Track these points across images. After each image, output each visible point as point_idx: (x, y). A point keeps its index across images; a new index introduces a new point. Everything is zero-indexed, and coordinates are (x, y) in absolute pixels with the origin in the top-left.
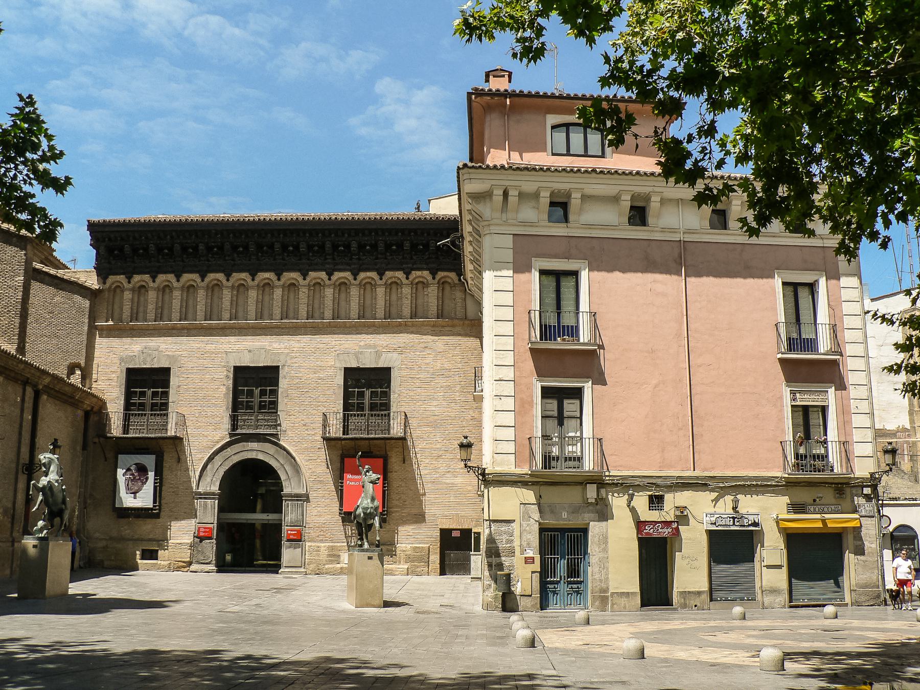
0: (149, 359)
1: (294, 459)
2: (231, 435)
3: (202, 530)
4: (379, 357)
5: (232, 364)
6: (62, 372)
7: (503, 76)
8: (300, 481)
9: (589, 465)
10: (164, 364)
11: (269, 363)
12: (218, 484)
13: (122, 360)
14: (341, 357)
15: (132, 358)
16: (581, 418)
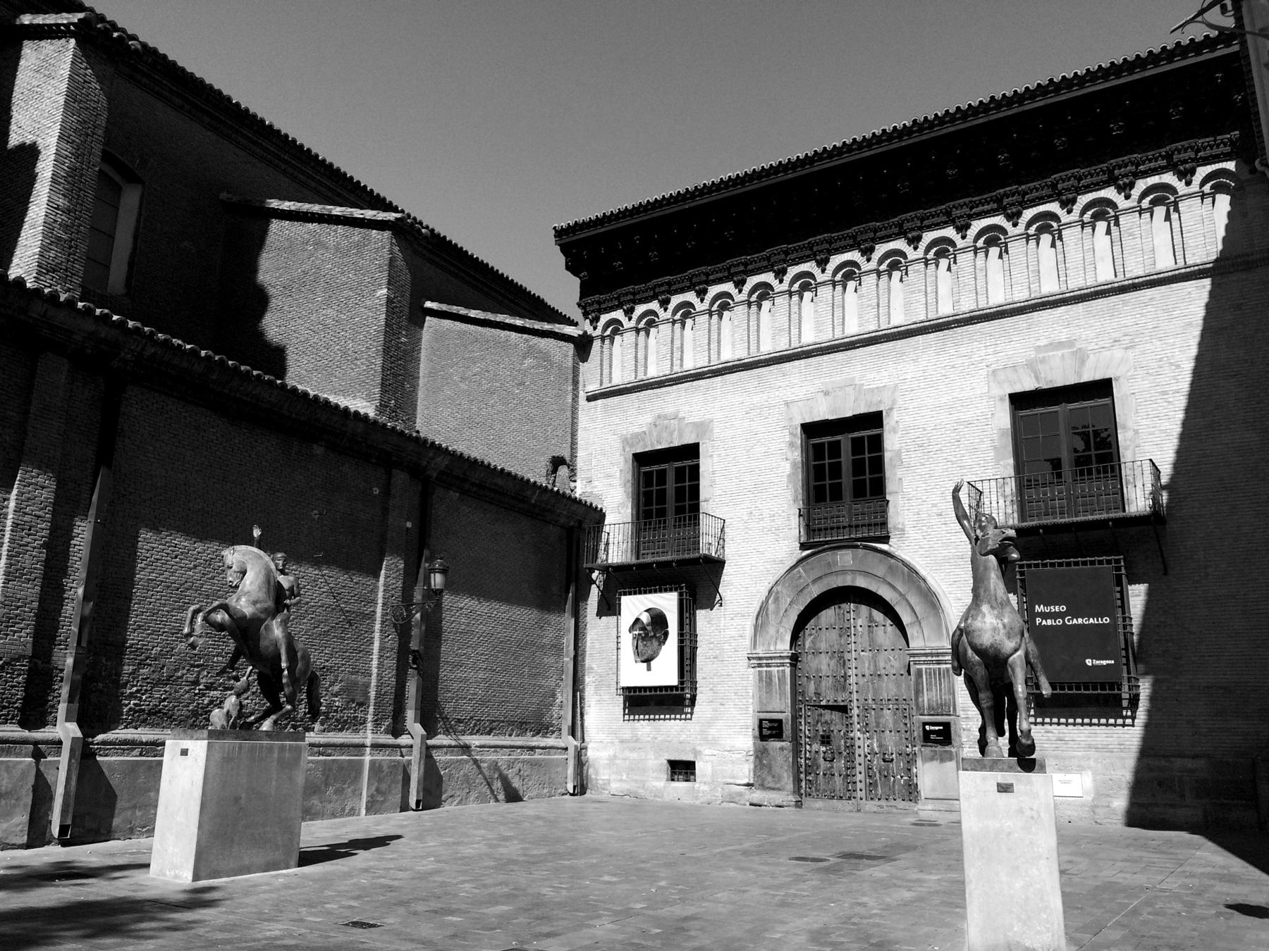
0: (665, 435)
2: (803, 546)
3: (766, 724)
4: (1083, 362)
6: (536, 473)
8: (940, 625)
11: (863, 409)
12: (788, 638)
13: (626, 441)
14: (1002, 376)
15: (639, 437)
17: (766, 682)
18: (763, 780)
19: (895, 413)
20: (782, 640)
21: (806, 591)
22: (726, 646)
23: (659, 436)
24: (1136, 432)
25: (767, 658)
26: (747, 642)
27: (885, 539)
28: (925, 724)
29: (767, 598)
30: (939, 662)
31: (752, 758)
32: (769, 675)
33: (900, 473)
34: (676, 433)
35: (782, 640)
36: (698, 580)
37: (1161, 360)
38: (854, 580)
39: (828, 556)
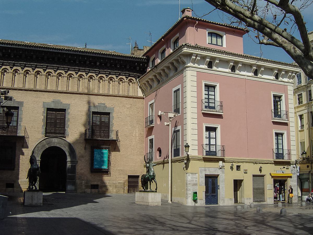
2: (46, 136)
7: (190, 11)
9: (219, 155)
16: (216, 138)
19: (69, 110)
20: (39, 157)
24: (113, 123)
27: (65, 137)
35: (39, 157)
37: (118, 111)
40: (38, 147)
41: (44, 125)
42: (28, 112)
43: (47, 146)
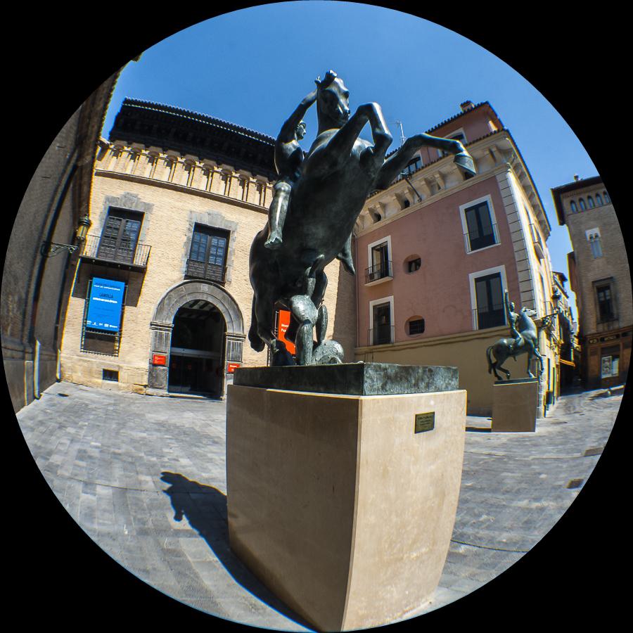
0: (128, 203)
1: (237, 305)
2: (187, 277)
5: (194, 221)
8: (240, 325)
10: (140, 209)
11: (222, 227)
12: (173, 318)
17: (159, 338)
18: (153, 384)
19: (236, 235)
21: (184, 298)
22: (139, 316)
23: (126, 202)
25: (160, 326)
26: (151, 316)
28: (230, 364)
29: (166, 296)
30: (238, 340)
31: (148, 373)
32: (161, 335)
33: (233, 258)
34: (134, 204)
35: (169, 319)
36: (130, 277)
38: (207, 298)
39: (198, 285)
40: (170, 299)
41: (186, 255)
42: (157, 225)
43: (189, 299)
